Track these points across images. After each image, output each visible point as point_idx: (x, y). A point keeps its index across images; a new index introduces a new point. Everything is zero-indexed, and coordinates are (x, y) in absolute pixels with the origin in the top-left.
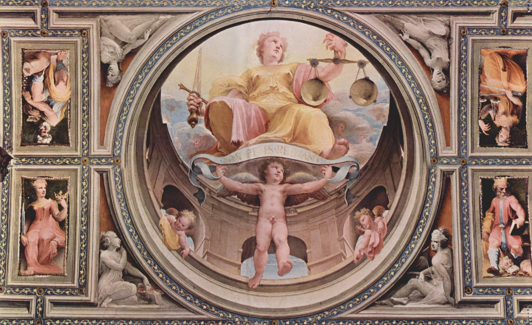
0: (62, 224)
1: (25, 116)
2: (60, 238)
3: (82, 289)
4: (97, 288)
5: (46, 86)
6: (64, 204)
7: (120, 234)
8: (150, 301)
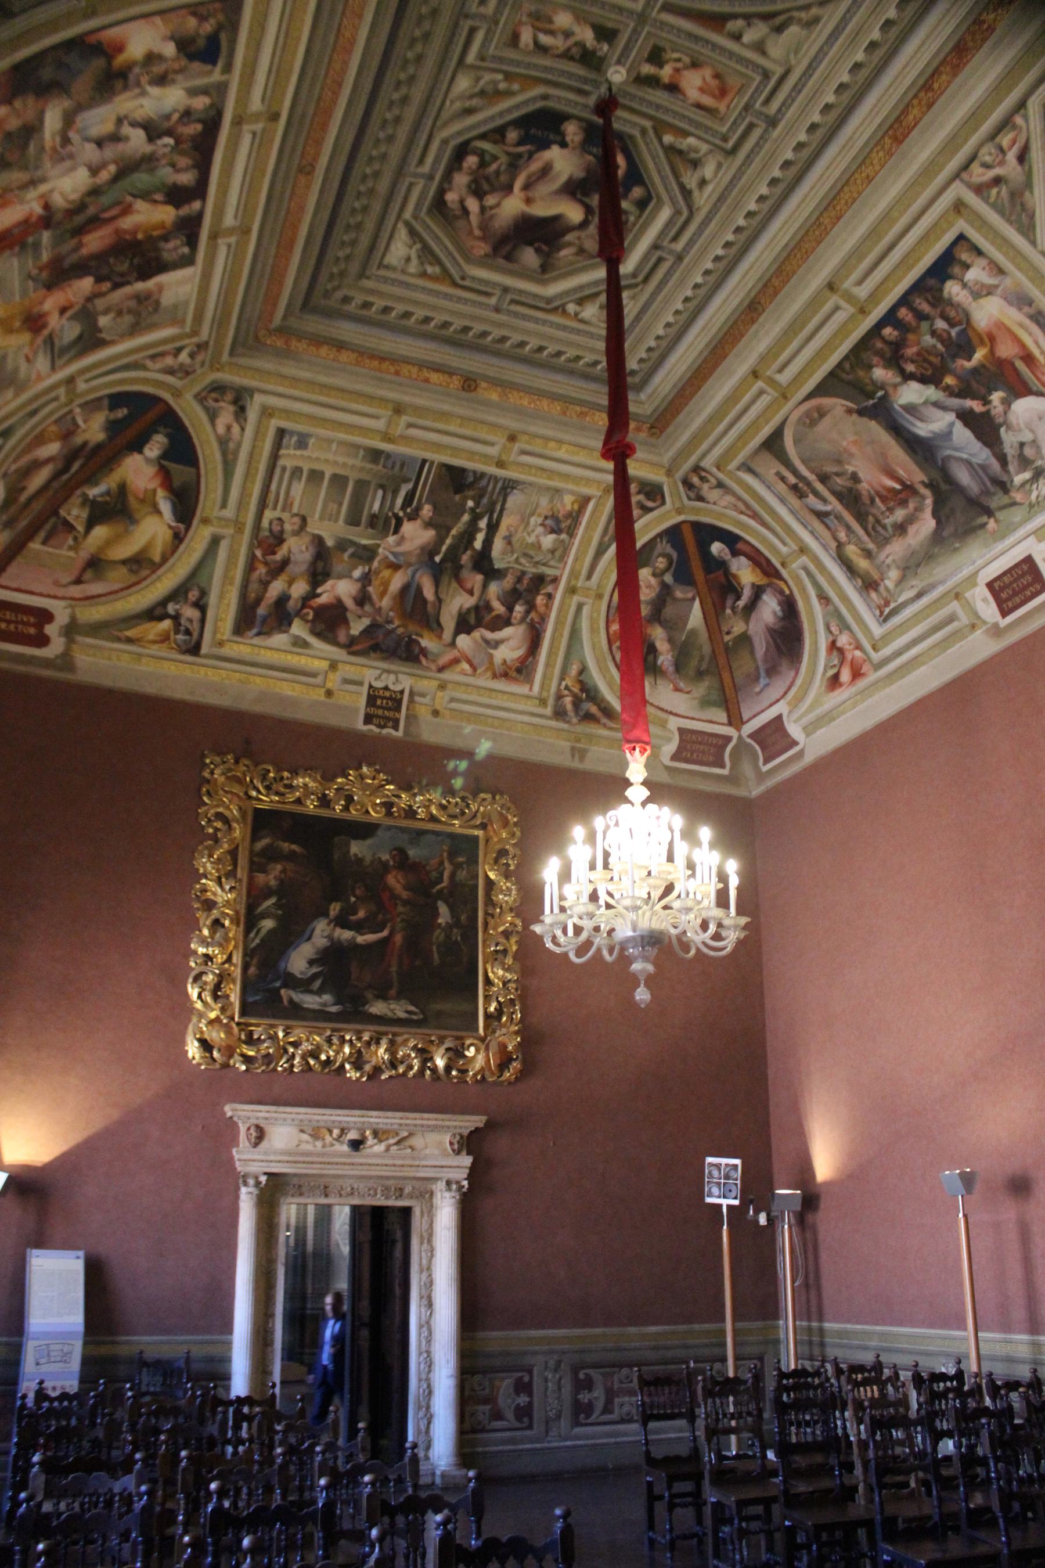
0: (695, 65)
1: (572, 59)
2: (707, 72)
3: (766, 75)
4: (774, 61)
5: (551, 33)
6: (676, 55)
7: (734, 16)
8: (816, 20)
